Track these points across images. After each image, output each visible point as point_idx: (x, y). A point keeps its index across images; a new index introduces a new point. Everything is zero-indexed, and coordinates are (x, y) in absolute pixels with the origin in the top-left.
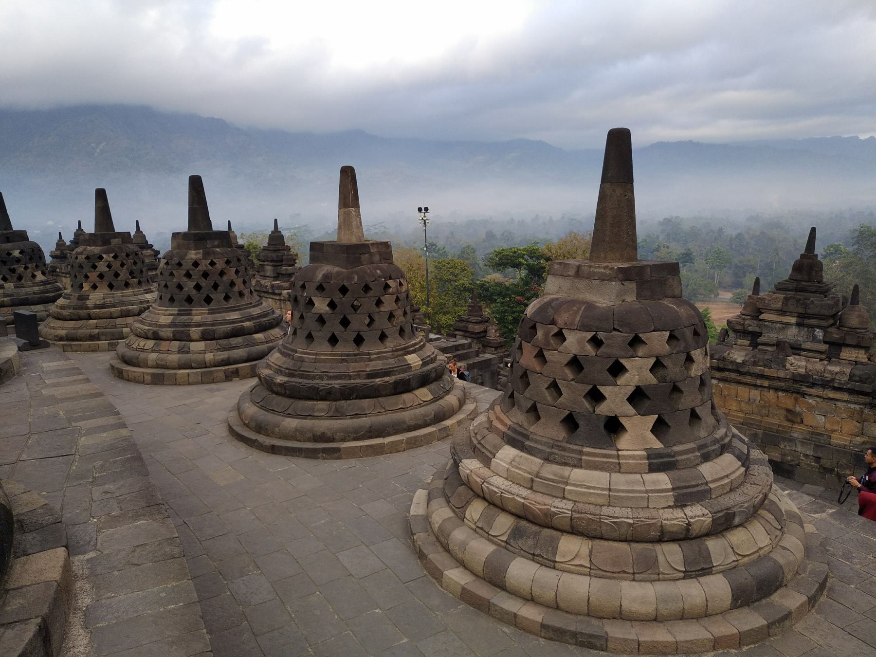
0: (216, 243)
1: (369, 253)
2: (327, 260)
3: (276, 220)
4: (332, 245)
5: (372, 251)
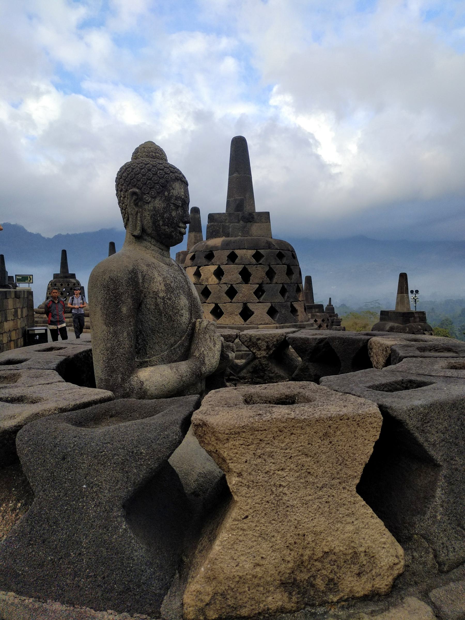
0: (317, 310)
1: (414, 317)
2: (390, 320)
3: (330, 299)
4: (394, 312)
5: (415, 316)
